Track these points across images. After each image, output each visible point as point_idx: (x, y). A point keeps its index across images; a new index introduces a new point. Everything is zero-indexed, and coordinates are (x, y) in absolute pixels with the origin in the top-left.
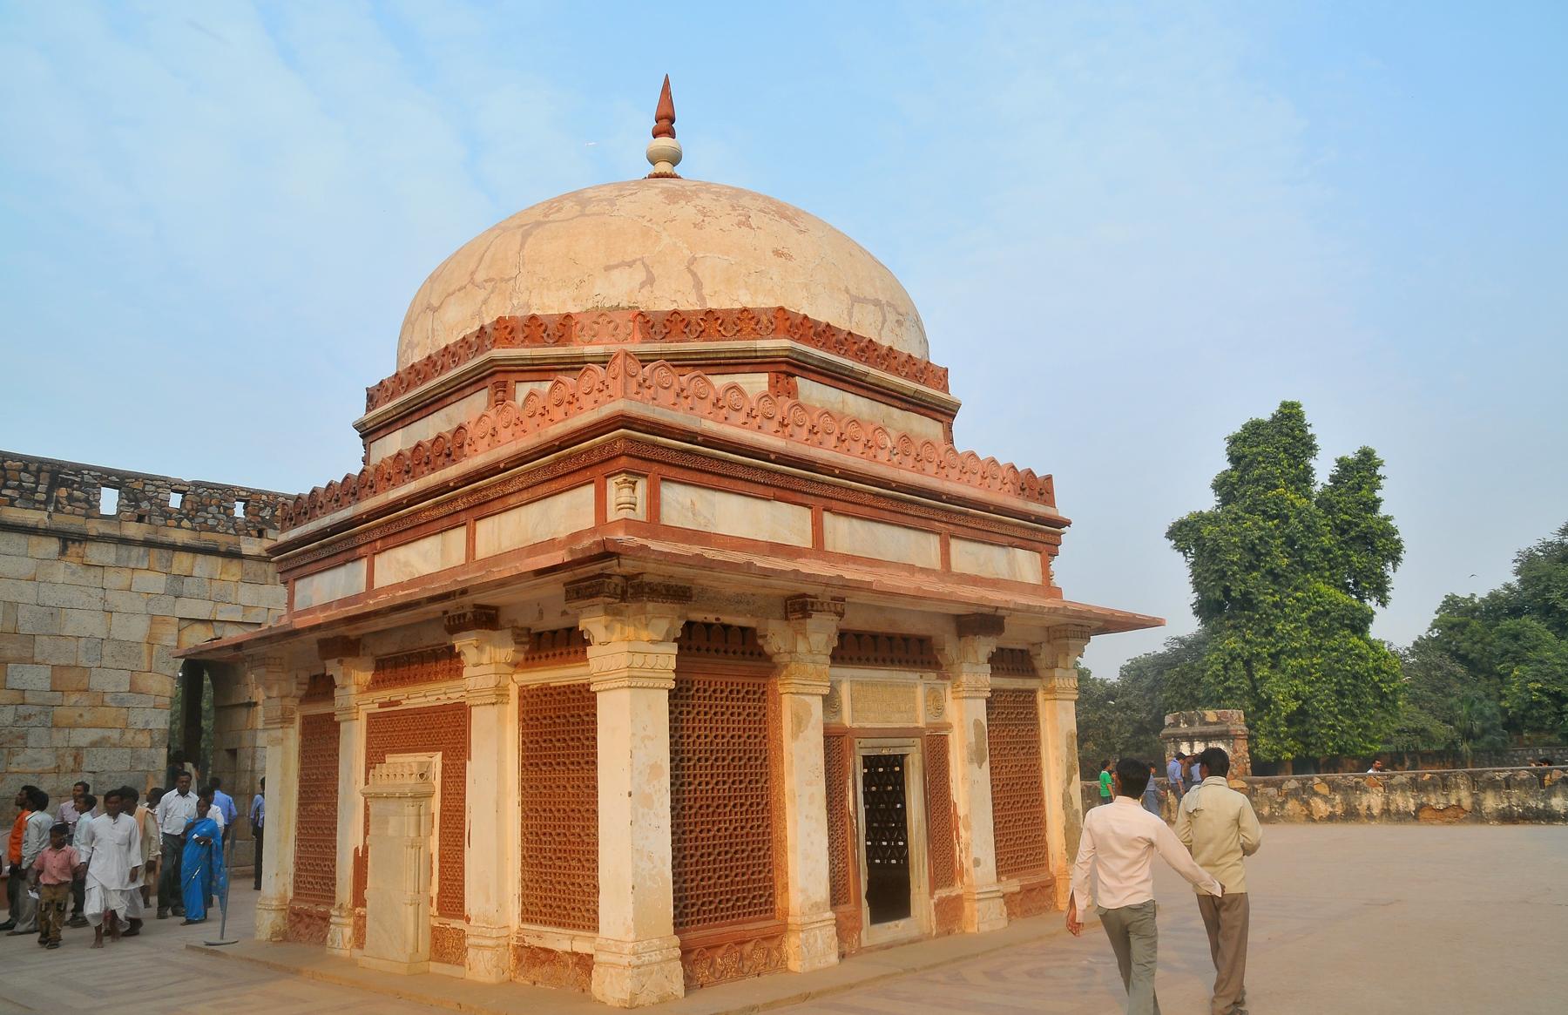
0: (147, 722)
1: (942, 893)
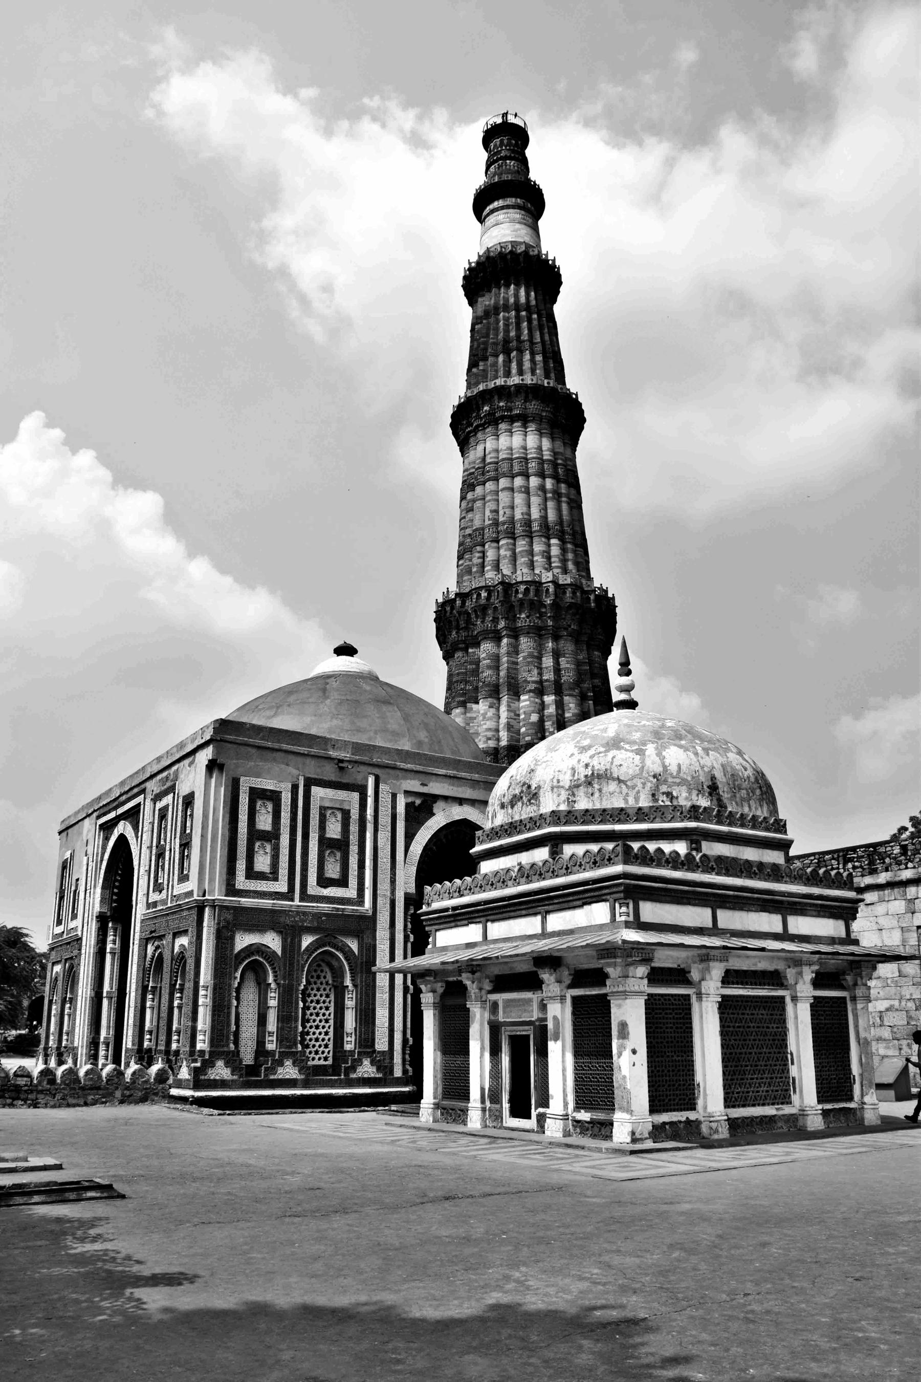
0: (911, 995)
1: (541, 1110)
